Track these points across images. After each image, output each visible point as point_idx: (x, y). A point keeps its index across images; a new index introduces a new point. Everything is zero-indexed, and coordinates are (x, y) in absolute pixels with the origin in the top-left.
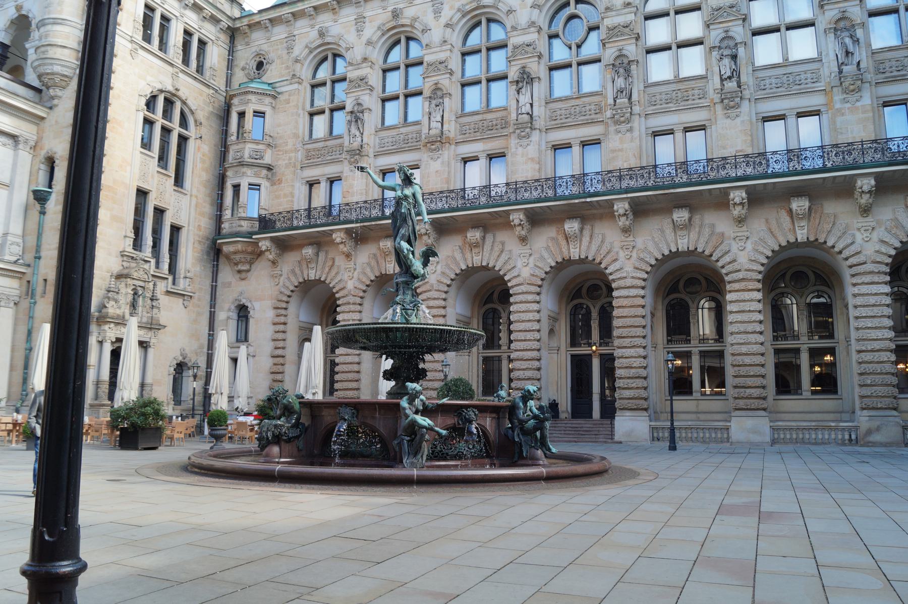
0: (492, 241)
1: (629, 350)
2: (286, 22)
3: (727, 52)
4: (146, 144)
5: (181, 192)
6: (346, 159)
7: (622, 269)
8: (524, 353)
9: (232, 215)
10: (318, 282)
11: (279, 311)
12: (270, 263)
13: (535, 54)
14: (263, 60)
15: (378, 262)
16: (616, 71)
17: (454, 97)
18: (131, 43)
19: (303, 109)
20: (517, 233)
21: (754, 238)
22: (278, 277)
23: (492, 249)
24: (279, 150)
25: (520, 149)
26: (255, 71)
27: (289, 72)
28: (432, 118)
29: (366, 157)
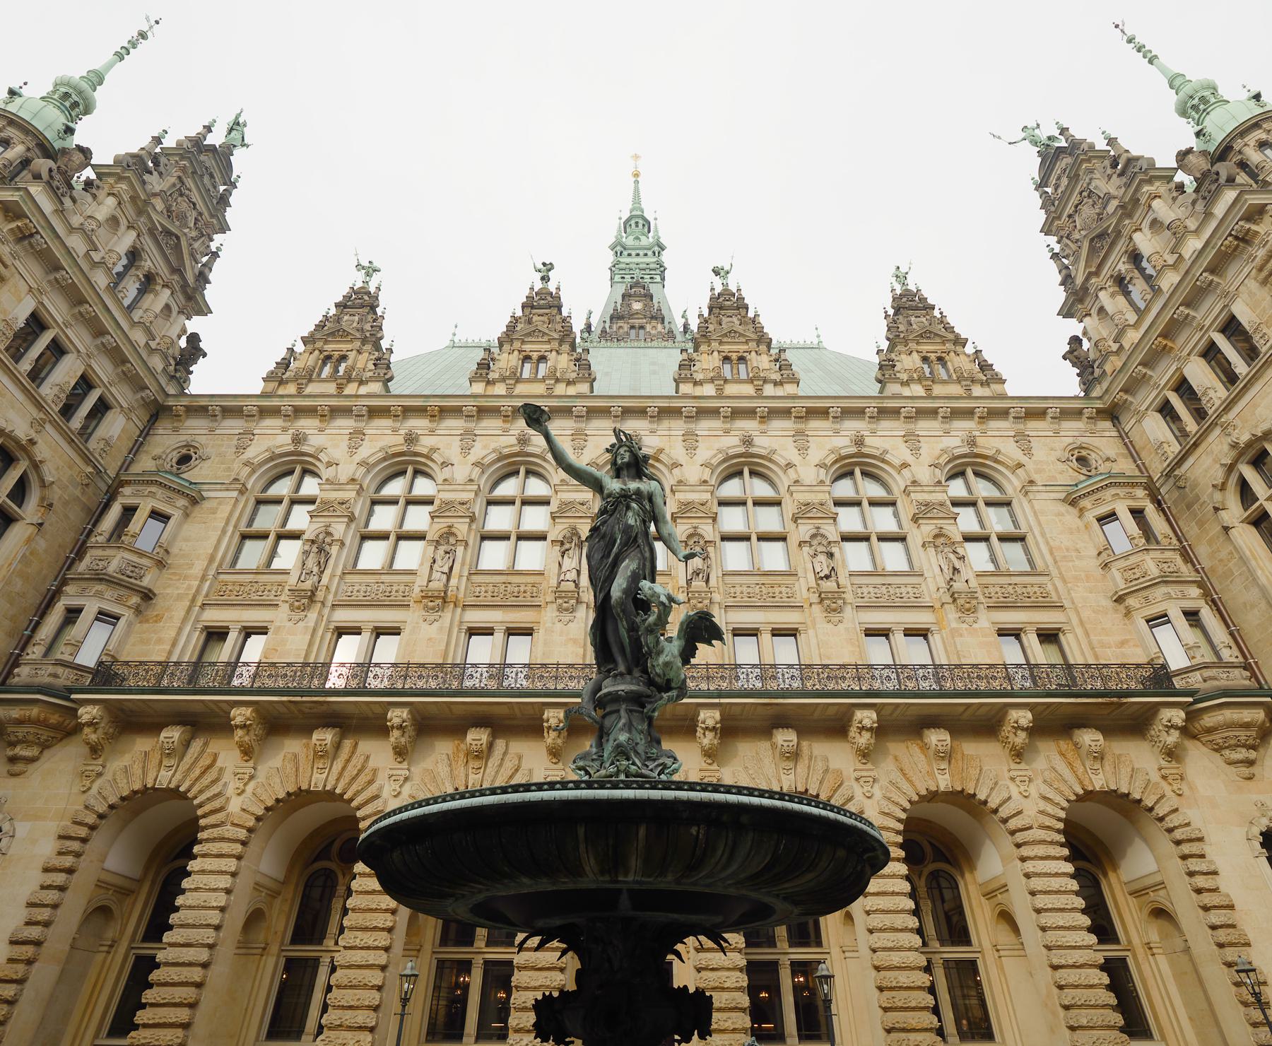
2: (247, 416)
3: (820, 549)
9: (46, 655)
10: (174, 793)
11: (68, 843)
12: (86, 749)
19: (235, 527)
21: (884, 782)
22: (92, 778)
23: (501, 765)
24: (174, 574)
25: (559, 625)
26: (174, 464)
28: (436, 567)
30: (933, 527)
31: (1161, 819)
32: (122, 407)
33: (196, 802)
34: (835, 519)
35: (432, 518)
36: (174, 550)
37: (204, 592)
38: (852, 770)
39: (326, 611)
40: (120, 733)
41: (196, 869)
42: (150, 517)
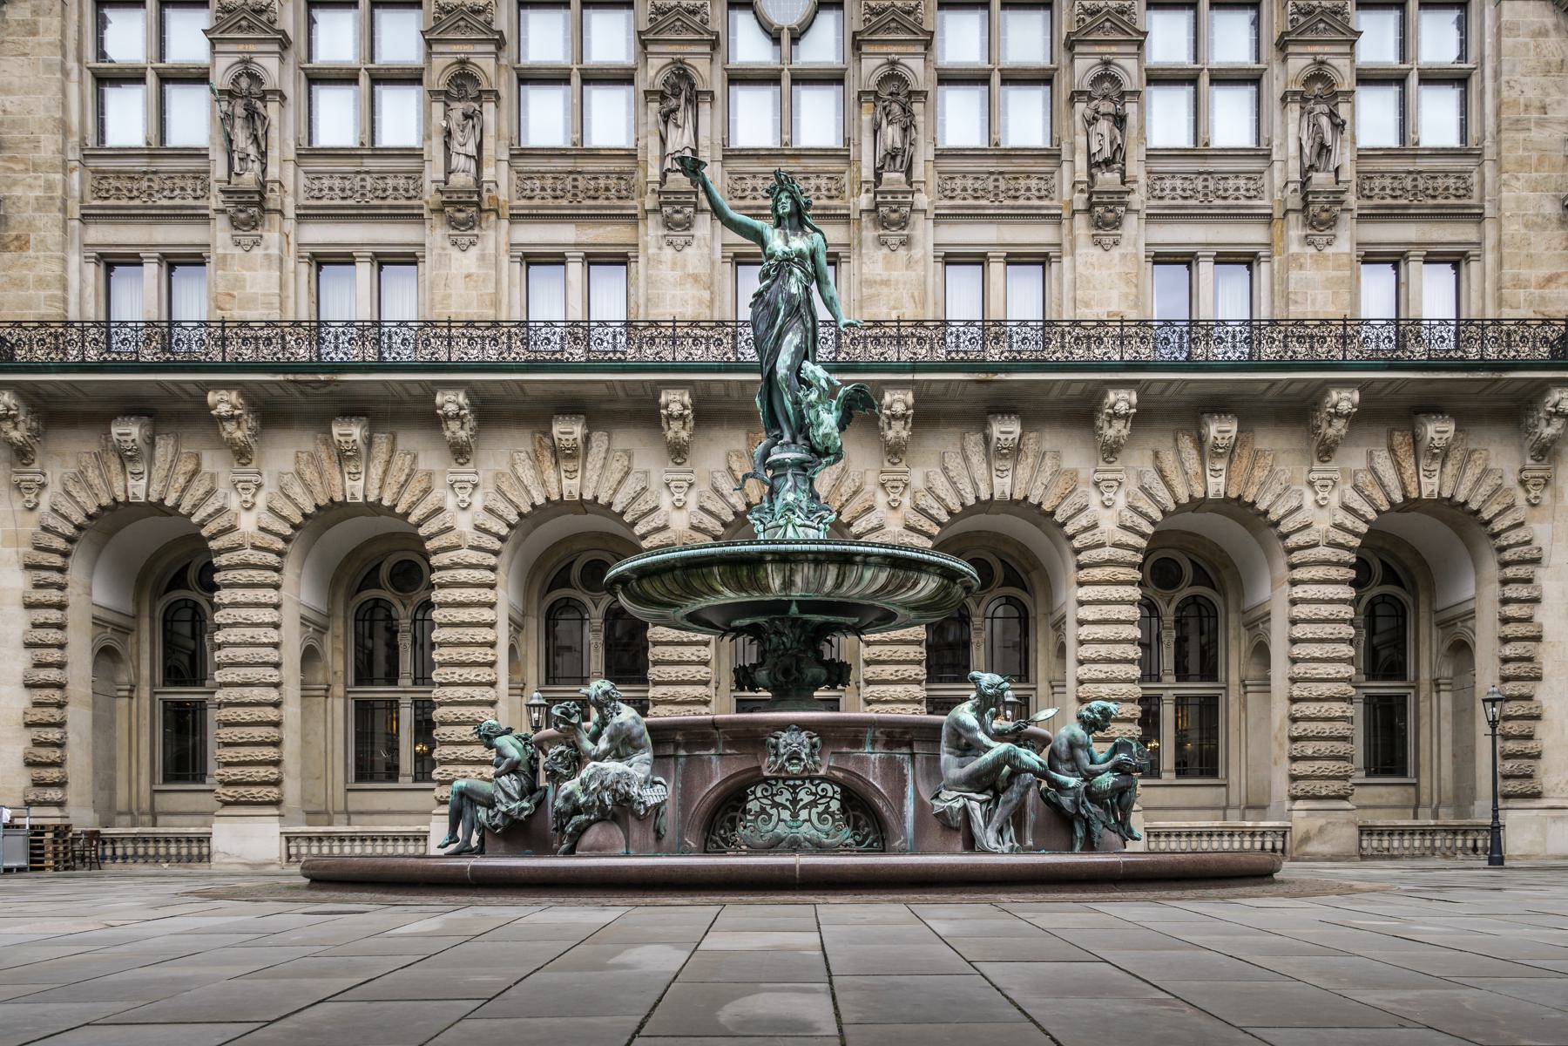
0: (605, 447)
1: (891, 688)
3: (1106, 107)
6: (223, 211)
7: (881, 527)
13: (706, 37)
16: (885, 108)
17: (504, 103)
24: (11, 159)
25: (669, 251)
28: (455, 146)
29: (277, 217)
30: (1308, 61)
31: (1496, 535)
34: (1140, 44)
35: (429, 43)
38: (1092, 470)
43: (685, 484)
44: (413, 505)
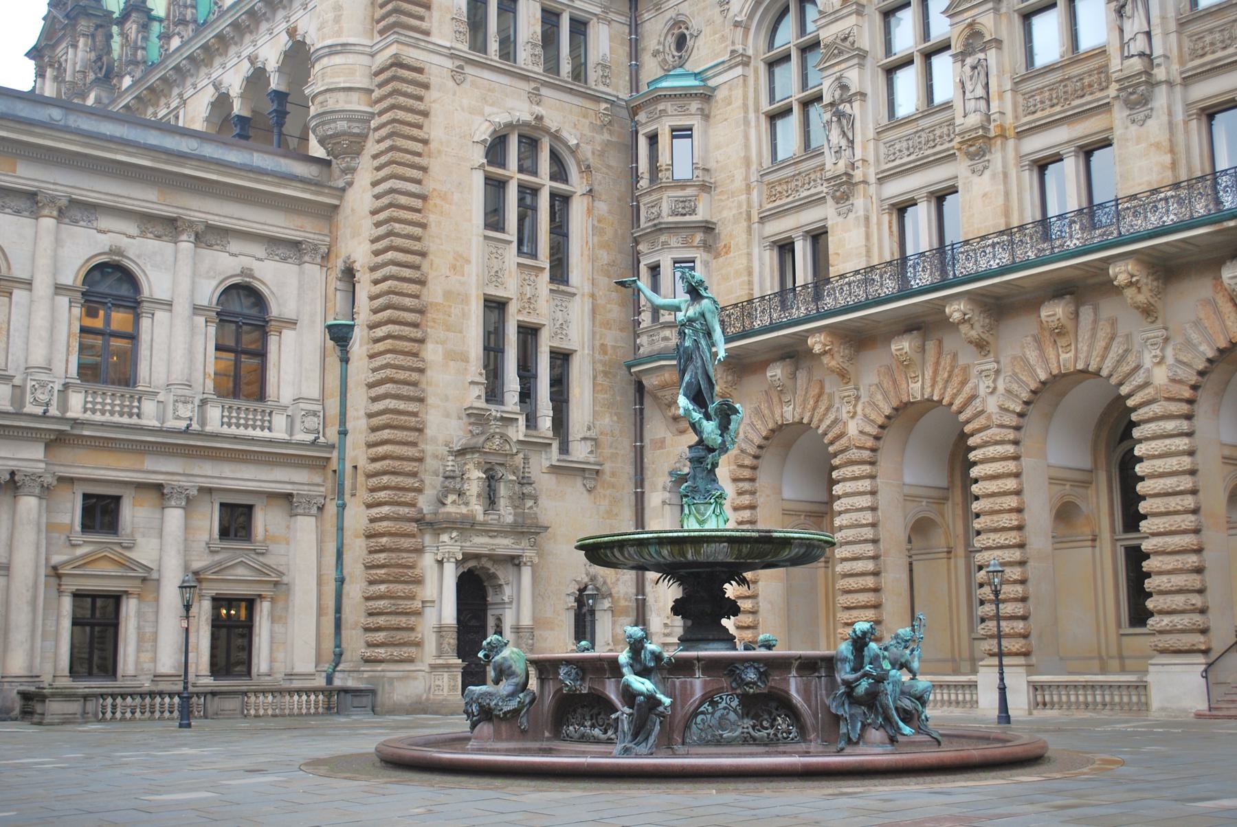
4: (494, 218)
5: (563, 292)
8: (1168, 539)
11: (741, 485)
14: (685, 31)
15: (895, 382)
17: (1006, 45)
18: (452, 58)
19: (757, 110)
20: (1129, 301)
23: (1093, 335)
25: (1134, 128)
26: (676, 54)
27: (726, 47)
28: (968, 95)
32: (595, 15)
33: (820, 431)
36: (712, 165)
37: (756, 204)
39: (872, 189)
40: (740, 377)
41: (840, 493)
42: (673, 137)
43: (1160, 340)
44: (954, 396)
